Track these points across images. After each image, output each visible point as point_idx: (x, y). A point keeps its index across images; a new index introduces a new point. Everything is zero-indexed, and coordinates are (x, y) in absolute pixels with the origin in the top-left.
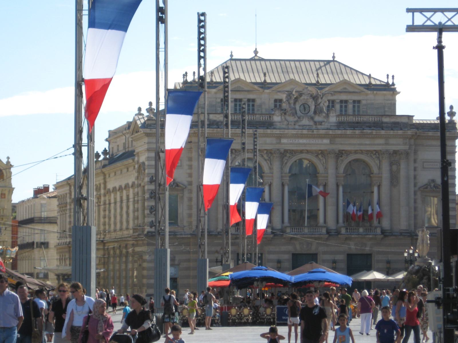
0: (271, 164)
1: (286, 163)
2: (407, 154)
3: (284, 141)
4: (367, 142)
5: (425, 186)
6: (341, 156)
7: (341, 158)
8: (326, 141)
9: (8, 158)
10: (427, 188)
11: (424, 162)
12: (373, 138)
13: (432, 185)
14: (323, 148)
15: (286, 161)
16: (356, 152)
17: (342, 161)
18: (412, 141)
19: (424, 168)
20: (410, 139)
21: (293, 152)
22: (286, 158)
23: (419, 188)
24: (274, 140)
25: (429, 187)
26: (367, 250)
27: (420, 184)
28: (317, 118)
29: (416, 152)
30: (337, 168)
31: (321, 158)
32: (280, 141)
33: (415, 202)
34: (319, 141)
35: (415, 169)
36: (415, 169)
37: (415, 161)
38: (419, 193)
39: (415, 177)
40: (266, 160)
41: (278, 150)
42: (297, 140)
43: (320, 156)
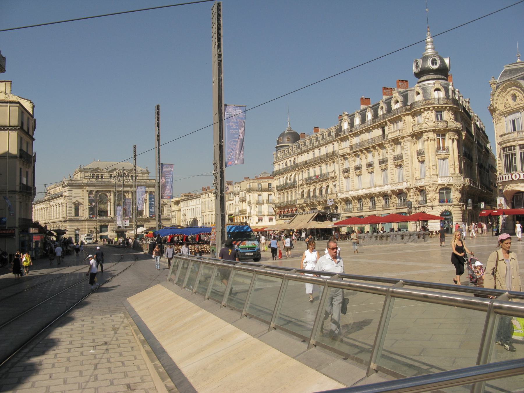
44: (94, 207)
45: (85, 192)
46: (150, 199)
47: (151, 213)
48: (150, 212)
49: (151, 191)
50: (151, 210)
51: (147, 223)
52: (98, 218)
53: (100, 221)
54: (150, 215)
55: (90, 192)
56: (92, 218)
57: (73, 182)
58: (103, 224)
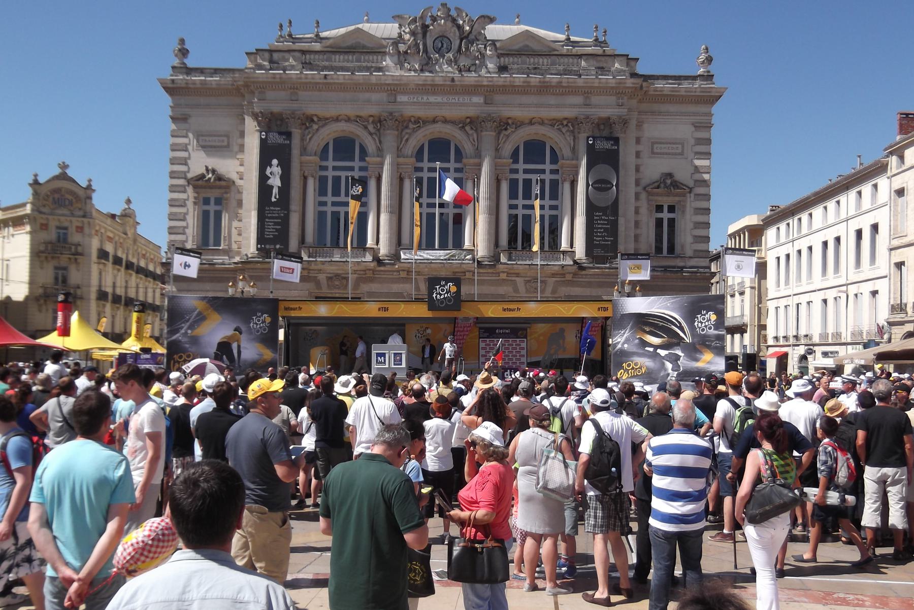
0: (380, 142)
1: (407, 140)
2: (625, 123)
3: (402, 98)
4: (552, 100)
5: (656, 184)
6: (506, 129)
7: (504, 132)
8: (478, 99)
9: (90, 181)
10: (658, 187)
11: (653, 143)
12: (562, 94)
13: (669, 182)
14: (472, 112)
15: (407, 137)
16: (531, 123)
17: (508, 136)
18: (634, 102)
19: (653, 153)
20: (630, 98)
21: (420, 122)
22: (408, 131)
23: (644, 188)
24: (383, 96)
25: (662, 185)
27: (644, 182)
29: (639, 126)
30: (497, 150)
31: (470, 132)
32: (396, 99)
33: (637, 212)
34: (466, 99)
35: (638, 155)
36: (638, 155)
37: (638, 140)
38: (643, 196)
39: (637, 169)
40: (371, 134)
41: (391, 114)
42: (425, 98)
43: (468, 128)
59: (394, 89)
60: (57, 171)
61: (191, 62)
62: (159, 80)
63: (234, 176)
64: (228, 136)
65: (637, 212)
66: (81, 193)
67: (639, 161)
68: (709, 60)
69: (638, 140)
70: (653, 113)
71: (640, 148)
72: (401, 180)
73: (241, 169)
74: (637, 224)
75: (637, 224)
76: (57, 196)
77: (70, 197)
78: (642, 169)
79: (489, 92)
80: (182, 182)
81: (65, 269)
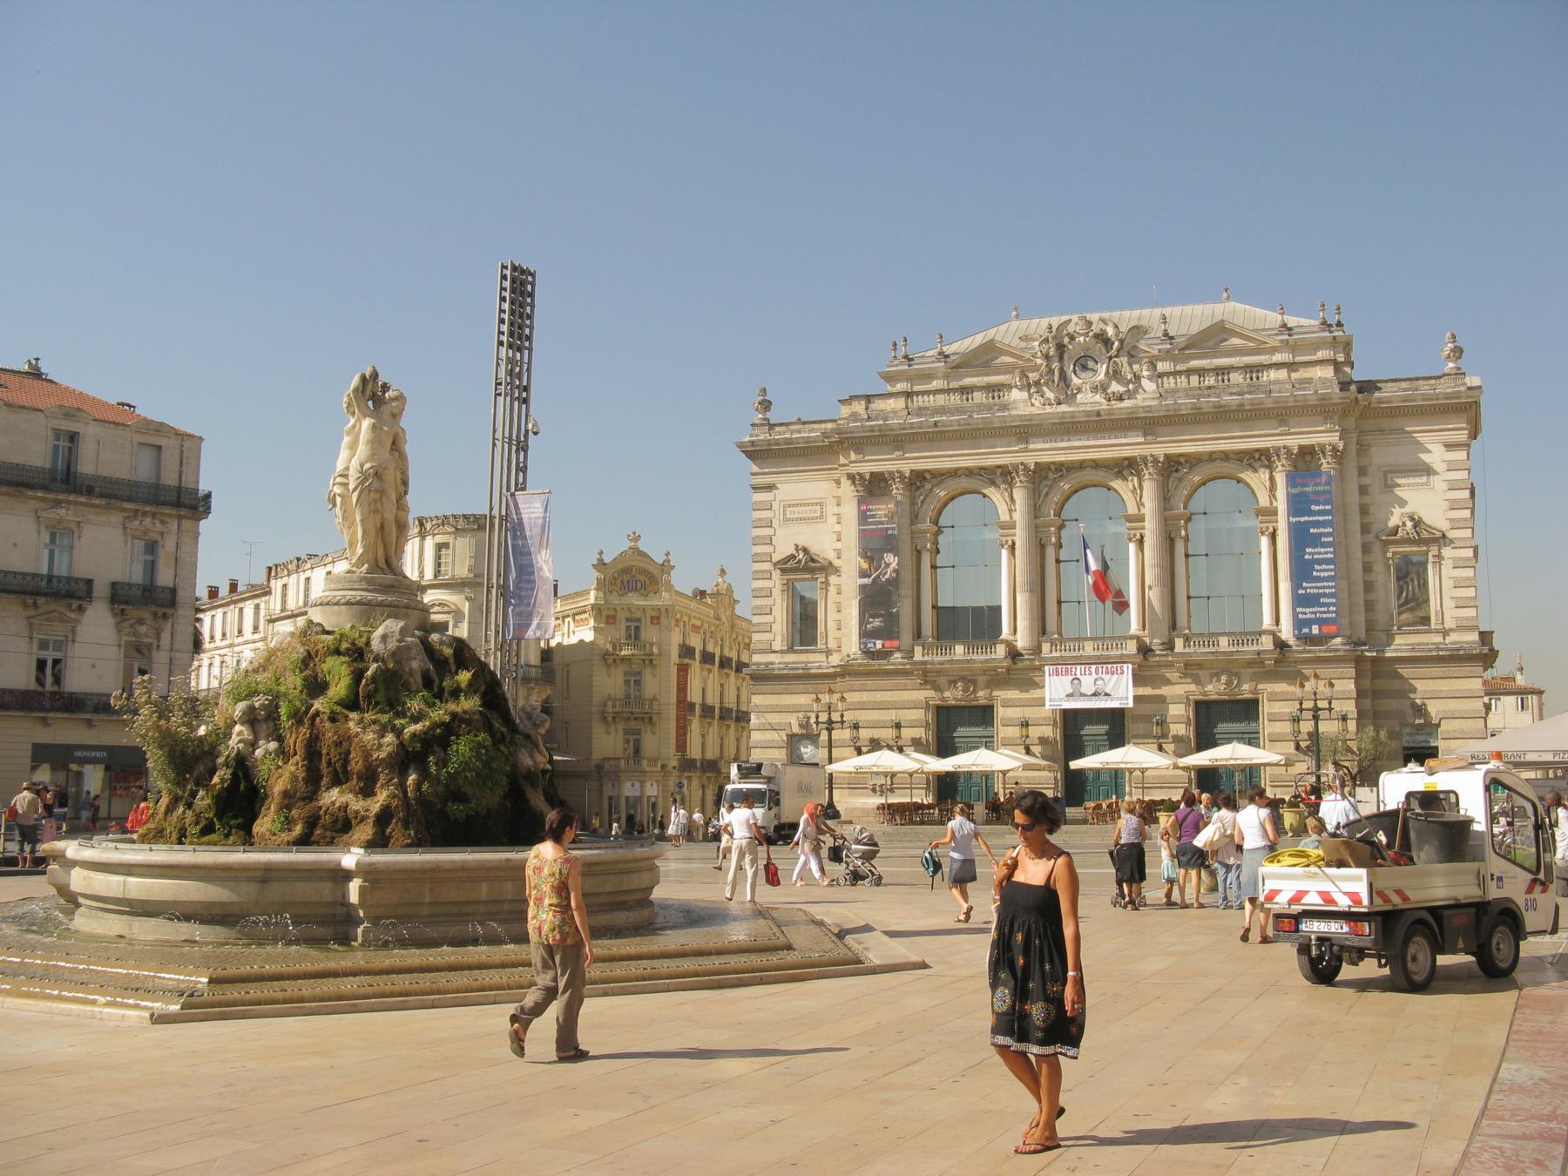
11: (1386, 473)
12: (1248, 419)
14: (1127, 452)
17: (1180, 480)
18: (1351, 422)
26: (1246, 690)
28: (1115, 387)
29: (1362, 449)
33: (1367, 568)
35: (1363, 490)
37: (1362, 471)
39: (1364, 510)
44: (894, 582)
45: (847, 490)
46: (1298, 505)
47: (1308, 613)
48: (1299, 601)
49: (1307, 453)
50: (1310, 588)
51: (1282, 687)
52: (918, 655)
53: (928, 677)
54: (1299, 624)
55: (873, 487)
56: (884, 654)
57: (780, 434)
58: (953, 696)
59: (1025, 431)
60: (626, 545)
61: (773, 416)
62: (740, 445)
63: (831, 556)
64: (821, 505)
65: (1367, 568)
66: (656, 572)
67: (1367, 500)
68: (1458, 352)
69: (1362, 471)
70: (1382, 431)
71: (1367, 481)
72: (1042, 547)
73: (839, 545)
74: (1368, 587)
75: (1368, 587)
76: (625, 578)
77: (642, 578)
78: (1373, 509)
79: (1149, 424)
80: (767, 566)
81: (639, 673)
